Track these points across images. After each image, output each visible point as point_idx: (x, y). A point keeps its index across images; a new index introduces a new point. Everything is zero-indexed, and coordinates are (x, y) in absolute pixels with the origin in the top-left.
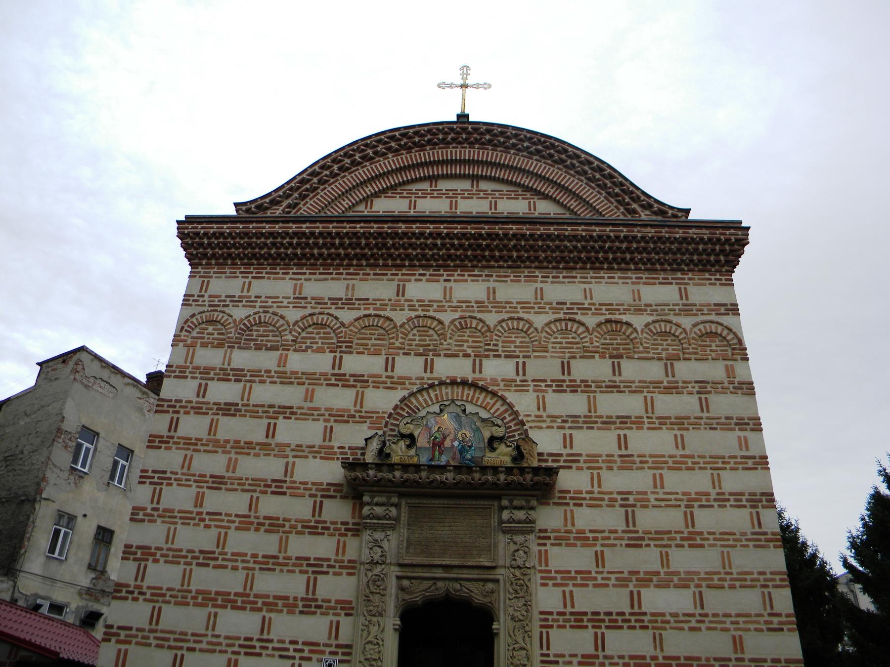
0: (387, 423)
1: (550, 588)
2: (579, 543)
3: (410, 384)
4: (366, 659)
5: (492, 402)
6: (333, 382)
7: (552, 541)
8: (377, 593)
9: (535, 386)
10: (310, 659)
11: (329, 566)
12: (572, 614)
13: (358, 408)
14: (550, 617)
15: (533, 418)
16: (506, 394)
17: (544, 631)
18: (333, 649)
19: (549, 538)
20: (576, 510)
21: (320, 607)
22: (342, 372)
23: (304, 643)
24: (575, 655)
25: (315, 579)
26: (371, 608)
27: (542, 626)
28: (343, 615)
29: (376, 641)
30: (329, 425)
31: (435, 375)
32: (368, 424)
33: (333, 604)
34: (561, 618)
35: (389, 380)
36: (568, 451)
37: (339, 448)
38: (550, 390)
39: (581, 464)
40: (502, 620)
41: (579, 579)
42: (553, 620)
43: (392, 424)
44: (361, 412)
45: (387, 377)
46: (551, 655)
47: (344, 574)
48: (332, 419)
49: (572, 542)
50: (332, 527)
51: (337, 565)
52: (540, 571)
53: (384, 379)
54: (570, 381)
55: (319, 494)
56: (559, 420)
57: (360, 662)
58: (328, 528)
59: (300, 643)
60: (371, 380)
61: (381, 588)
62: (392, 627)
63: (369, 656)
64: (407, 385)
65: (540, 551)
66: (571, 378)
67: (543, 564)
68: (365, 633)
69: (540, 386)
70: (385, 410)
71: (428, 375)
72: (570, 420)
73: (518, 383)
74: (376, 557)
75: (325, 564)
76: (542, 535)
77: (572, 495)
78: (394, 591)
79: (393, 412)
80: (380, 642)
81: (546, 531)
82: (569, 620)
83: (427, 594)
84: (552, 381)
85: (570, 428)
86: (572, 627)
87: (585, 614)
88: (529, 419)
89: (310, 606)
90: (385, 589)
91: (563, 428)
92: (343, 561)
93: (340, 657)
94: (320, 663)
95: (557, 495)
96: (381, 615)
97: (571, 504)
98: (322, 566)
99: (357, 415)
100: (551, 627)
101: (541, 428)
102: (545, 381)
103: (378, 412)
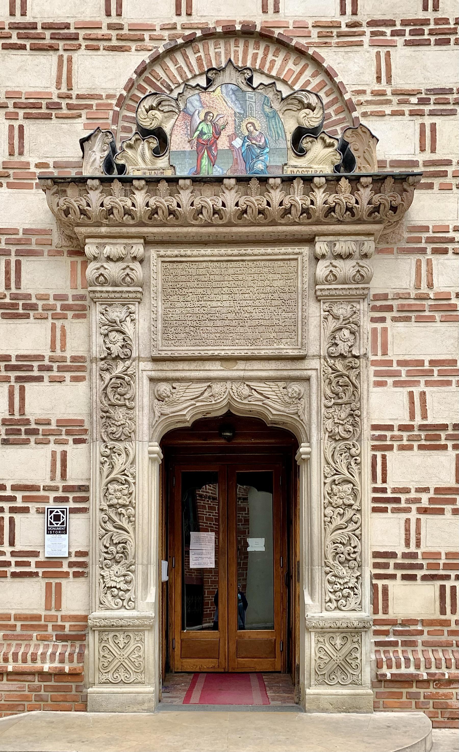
0: (116, 115)
1: (390, 388)
2: (438, 315)
3: (151, 39)
4: (110, 506)
5: (297, 69)
6: (14, 40)
7: (395, 314)
8: (121, 406)
9: (373, 34)
10: (26, 510)
11: (41, 368)
12: (422, 427)
13: (64, 89)
14: (389, 434)
15: (368, 97)
16: (323, 52)
17: (379, 454)
18: (60, 494)
19: (390, 308)
20: (437, 260)
21: (35, 432)
22: (28, 19)
23: (15, 488)
24: (426, 490)
25: (22, 389)
26: (114, 429)
27: (374, 448)
28: (71, 442)
29: (123, 478)
30: (16, 124)
31: (195, 19)
32: (83, 119)
33: (53, 426)
34: (405, 434)
35: (114, 33)
36: (428, 156)
37: (38, 166)
38: (400, 40)
39: (449, 180)
40: (314, 440)
41: (436, 373)
42: (393, 438)
43: (126, 118)
44: (69, 97)
45: (110, 27)
46: (389, 491)
47: (68, 379)
48: (21, 113)
49: (427, 313)
50: (40, 304)
51: (55, 365)
52: (374, 363)
53: (105, 31)
54: (437, 21)
55: (13, 249)
56: (414, 100)
57: (102, 510)
58: (34, 307)
59: (9, 488)
60: (82, 33)
61: (127, 396)
62: (147, 456)
63: (115, 501)
64: (148, 43)
65: (374, 330)
66: (439, 15)
67: (379, 353)
68: (106, 466)
69: (383, 34)
70: (112, 92)
71: (184, 19)
72: (433, 98)
73: (344, 29)
74: (116, 349)
75: (36, 364)
76: (378, 303)
77: (430, 234)
78: (146, 401)
79: (125, 93)
80: (130, 479)
81: (385, 297)
82: (418, 438)
83: (198, 404)
84: (405, 23)
85: (432, 113)
86: (421, 447)
87: (444, 427)
88: (362, 98)
89: (18, 432)
90: (132, 399)
91: (420, 114)
92: (63, 359)
93: (71, 505)
94: (42, 516)
95: (406, 235)
96: (128, 438)
97: (429, 251)
98: (30, 368)
99: (64, 103)
100: (390, 448)
101: (382, 115)
102: (391, 23)
103: (99, 97)
